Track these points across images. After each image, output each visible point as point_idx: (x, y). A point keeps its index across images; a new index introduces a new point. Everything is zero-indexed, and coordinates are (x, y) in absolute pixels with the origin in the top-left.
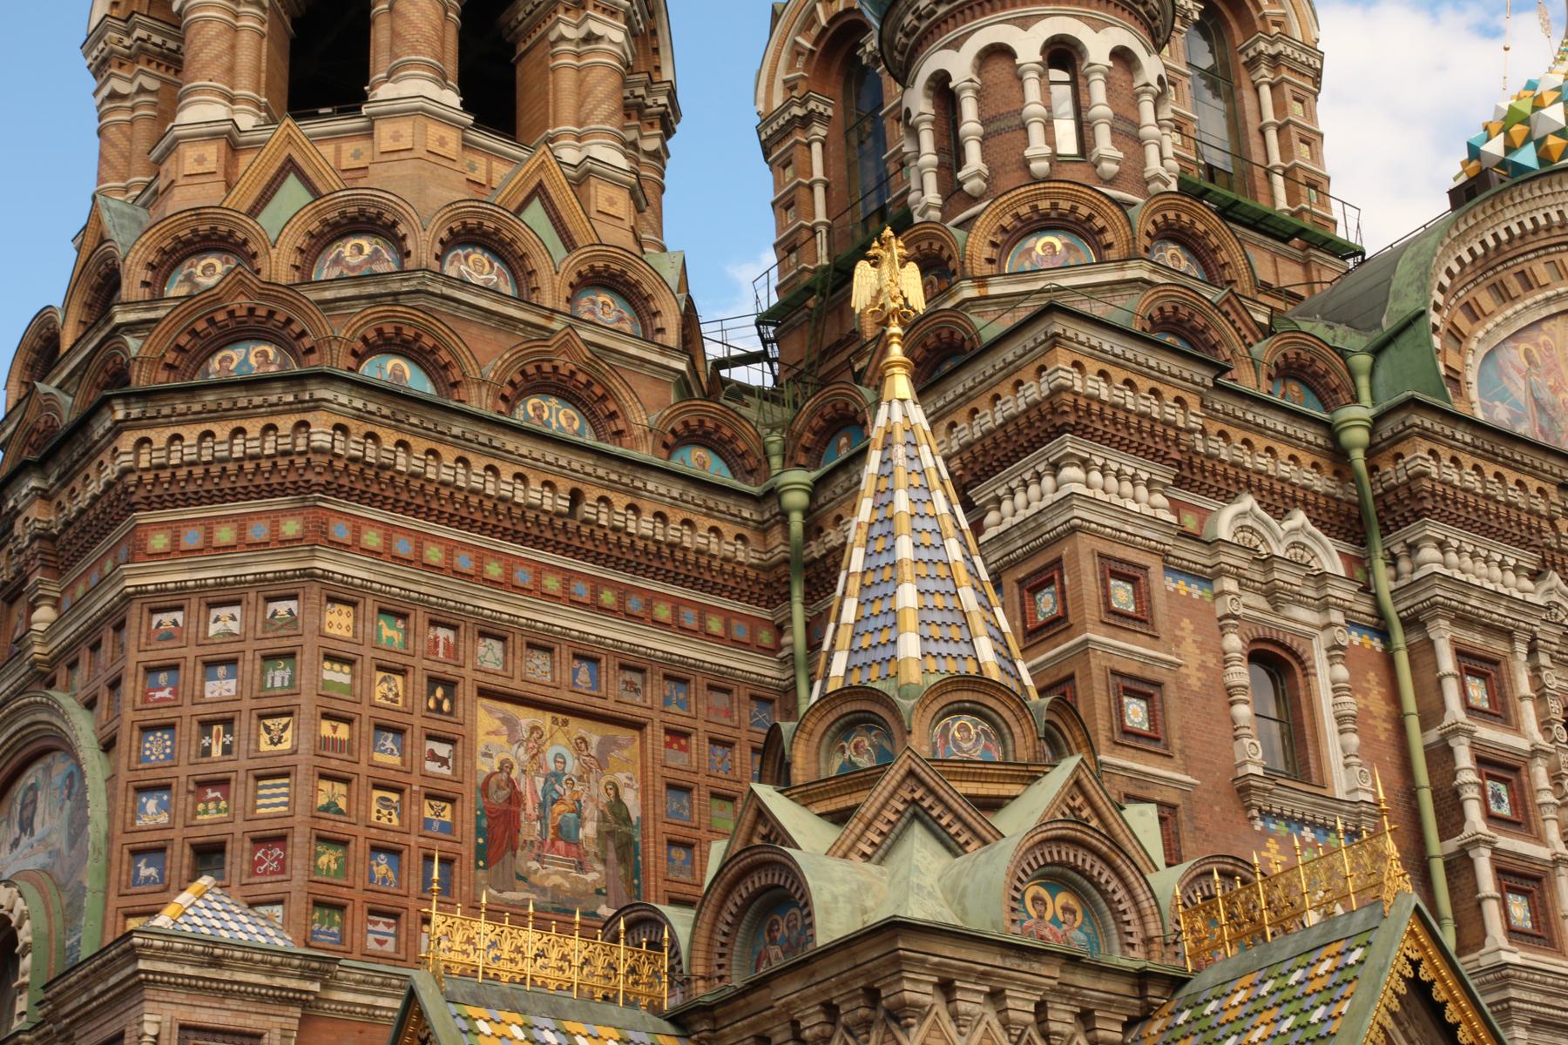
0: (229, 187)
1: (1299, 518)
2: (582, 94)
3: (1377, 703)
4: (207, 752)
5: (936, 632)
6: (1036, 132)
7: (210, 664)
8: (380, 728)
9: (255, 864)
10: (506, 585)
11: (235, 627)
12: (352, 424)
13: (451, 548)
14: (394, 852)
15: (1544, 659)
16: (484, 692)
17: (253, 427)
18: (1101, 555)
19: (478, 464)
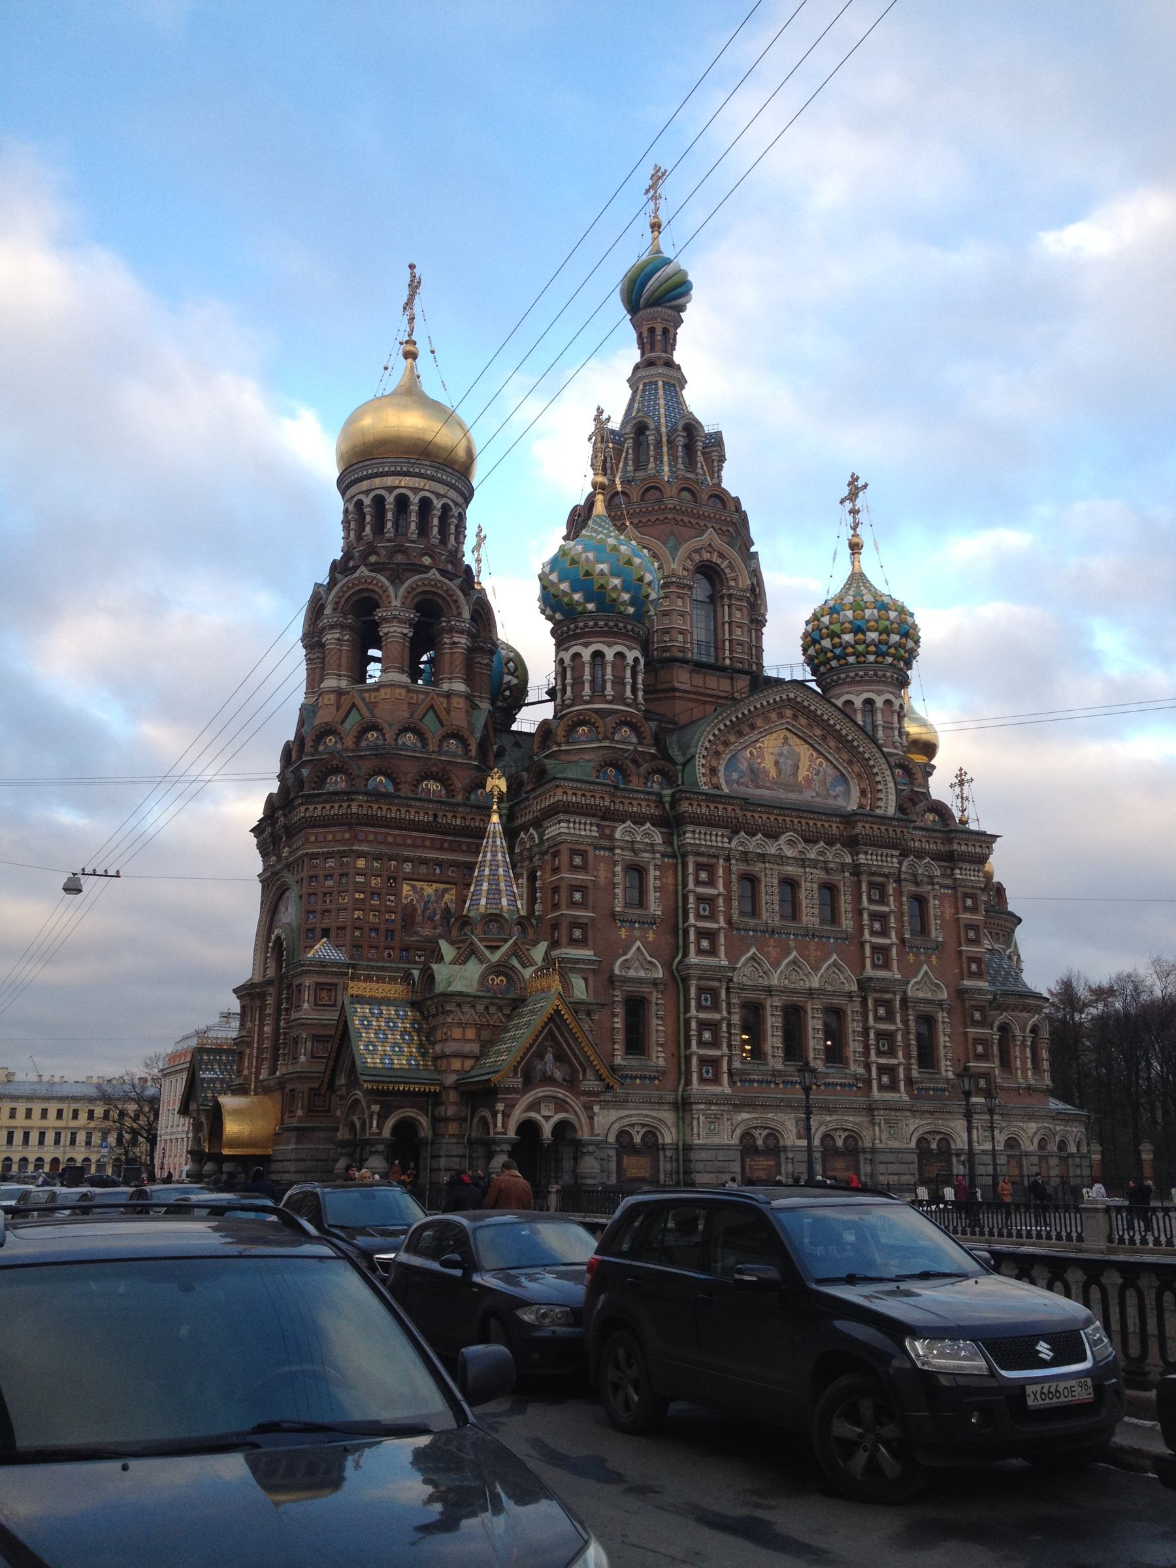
0: (338, 709)
1: (648, 825)
2: (452, 663)
3: (670, 880)
4: (325, 902)
5: (491, 896)
6: (587, 686)
7: (326, 876)
8: (373, 894)
9: (337, 935)
10: (413, 846)
11: (332, 865)
12: (364, 804)
13: (395, 836)
14: (377, 930)
15: (733, 861)
17: (336, 806)
18: (571, 849)
19: (403, 810)
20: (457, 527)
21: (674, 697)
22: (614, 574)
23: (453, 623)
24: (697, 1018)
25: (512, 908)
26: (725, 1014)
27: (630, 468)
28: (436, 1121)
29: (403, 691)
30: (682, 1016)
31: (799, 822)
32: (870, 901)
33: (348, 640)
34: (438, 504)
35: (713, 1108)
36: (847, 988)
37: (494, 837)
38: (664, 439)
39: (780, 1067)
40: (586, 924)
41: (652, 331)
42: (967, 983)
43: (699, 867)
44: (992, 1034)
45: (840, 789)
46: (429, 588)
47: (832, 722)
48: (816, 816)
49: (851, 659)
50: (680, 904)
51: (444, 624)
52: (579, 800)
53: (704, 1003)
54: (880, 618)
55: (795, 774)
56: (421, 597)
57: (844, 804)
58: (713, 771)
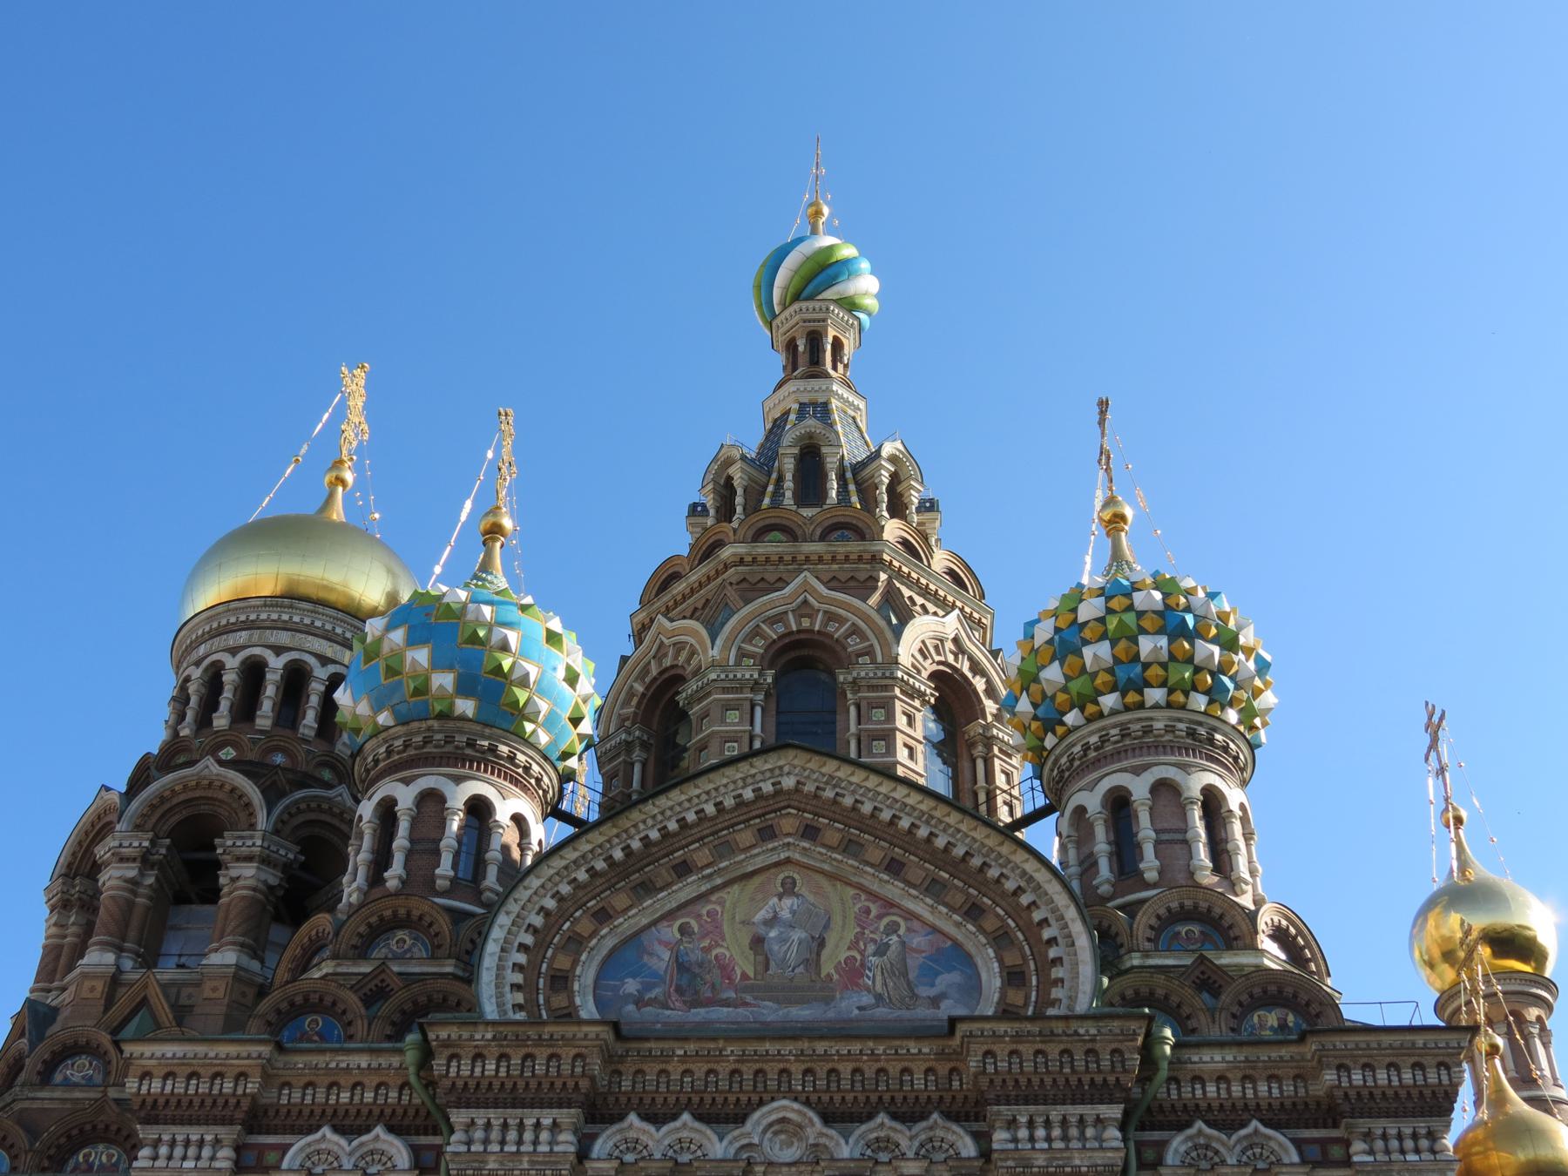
23: (229, 843)
29: (100, 986)
31: (807, 1072)
33: (73, 924)
38: (774, 476)
41: (791, 346)
45: (948, 980)
46: (198, 794)
47: (905, 823)
48: (856, 1047)
51: (219, 851)
52: (180, 1090)
54: (1110, 611)
55: (812, 961)
56: (185, 813)
57: (960, 1011)
58: (561, 981)
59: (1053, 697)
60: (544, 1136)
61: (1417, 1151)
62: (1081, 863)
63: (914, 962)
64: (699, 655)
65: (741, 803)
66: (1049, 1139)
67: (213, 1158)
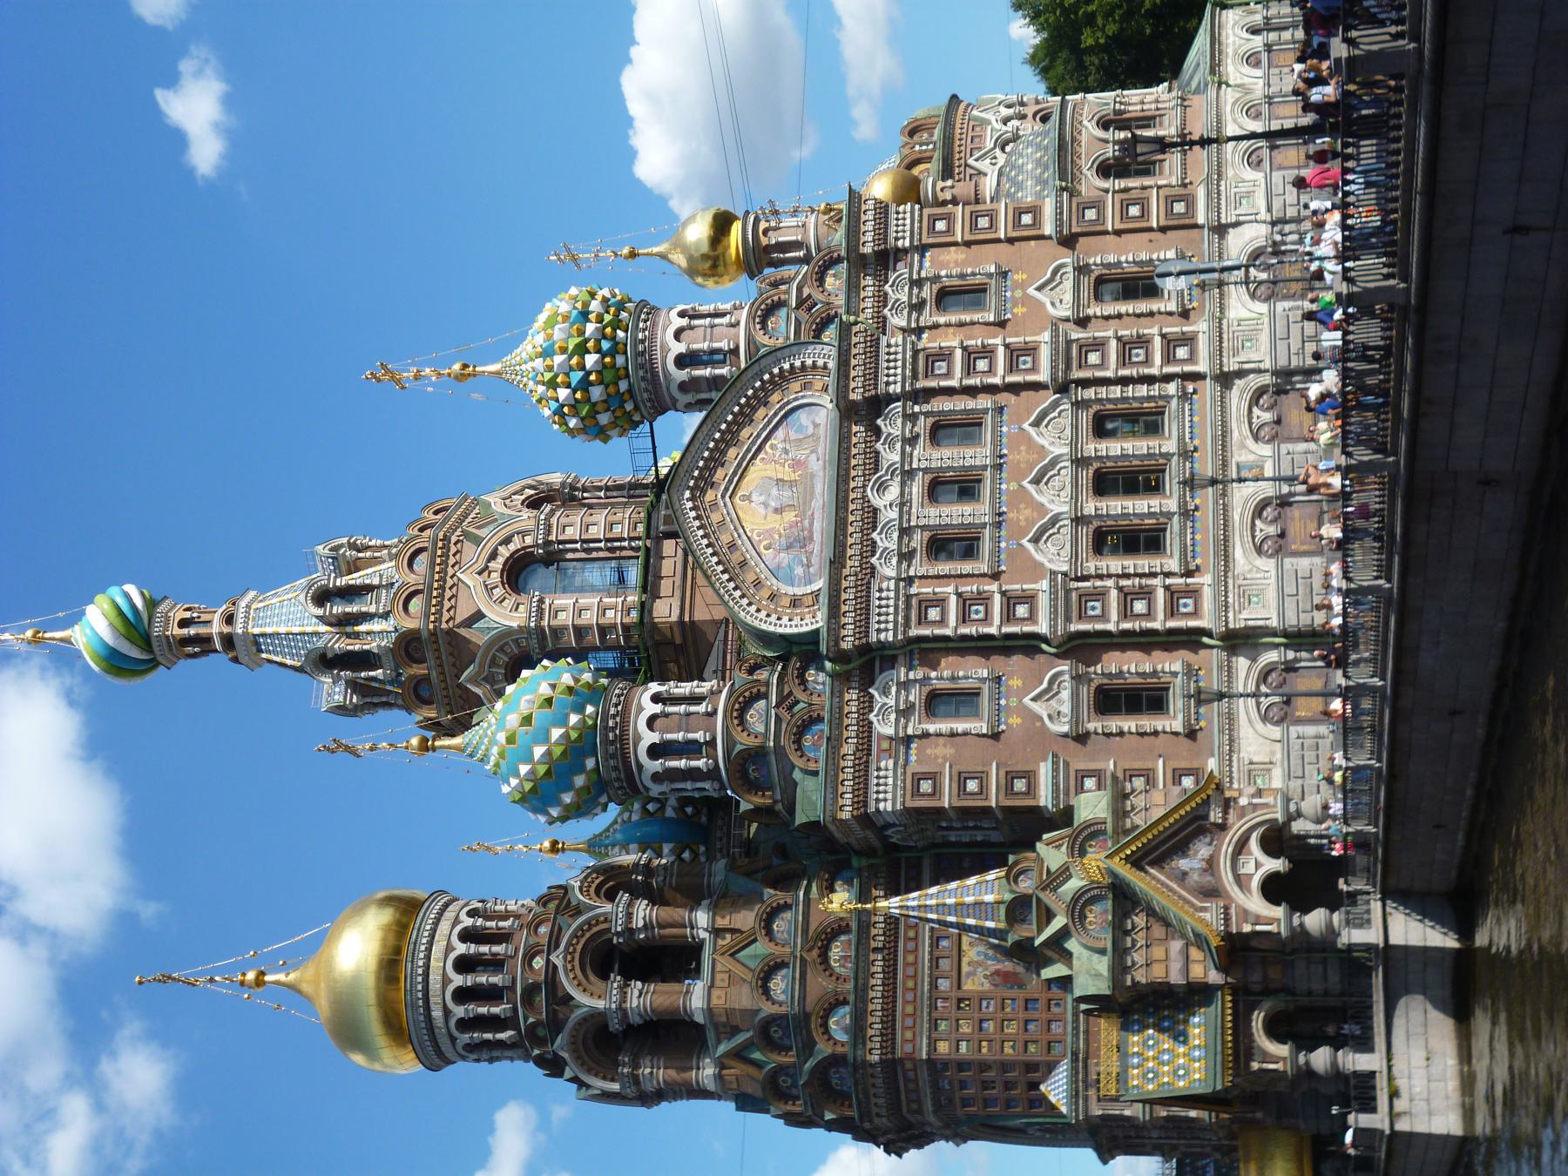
5: (983, 915)
6: (694, 763)
9: (1037, 1071)
13: (906, 1002)
14: (1027, 1022)
15: (912, 573)
16: (959, 987)
20: (488, 918)
21: (692, 622)
22: (546, 739)
23: (619, 929)
24: (1118, 622)
25: (996, 888)
26: (1110, 583)
27: (379, 673)
28: (1267, 992)
30: (1115, 640)
32: (948, 375)
34: (461, 948)
35: (1230, 600)
36: (1068, 406)
37: (907, 908)
39: (1172, 504)
40: (1007, 773)
42: (1048, 228)
43: (922, 620)
44: (1114, 192)
46: (577, 962)
48: (843, 456)
49: (623, 386)
50: (972, 644)
53: (1098, 612)
55: (792, 483)
56: (589, 972)
57: (823, 412)
58: (795, 602)
59: (608, 395)
60: (884, 595)
61: (904, 219)
62: (710, 391)
63: (793, 435)
64: (507, 643)
65: (698, 518)
66: (895, 368)
67: (887, 769)
